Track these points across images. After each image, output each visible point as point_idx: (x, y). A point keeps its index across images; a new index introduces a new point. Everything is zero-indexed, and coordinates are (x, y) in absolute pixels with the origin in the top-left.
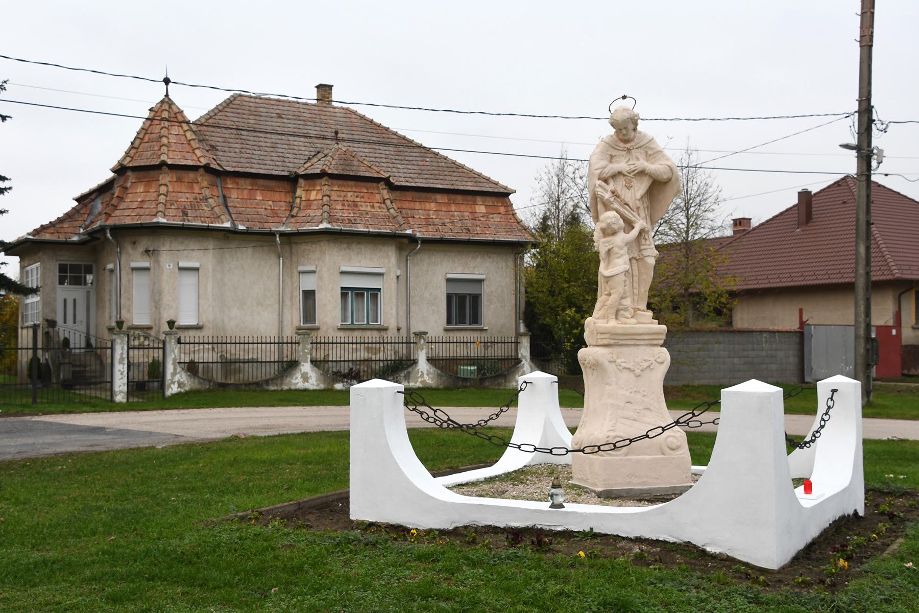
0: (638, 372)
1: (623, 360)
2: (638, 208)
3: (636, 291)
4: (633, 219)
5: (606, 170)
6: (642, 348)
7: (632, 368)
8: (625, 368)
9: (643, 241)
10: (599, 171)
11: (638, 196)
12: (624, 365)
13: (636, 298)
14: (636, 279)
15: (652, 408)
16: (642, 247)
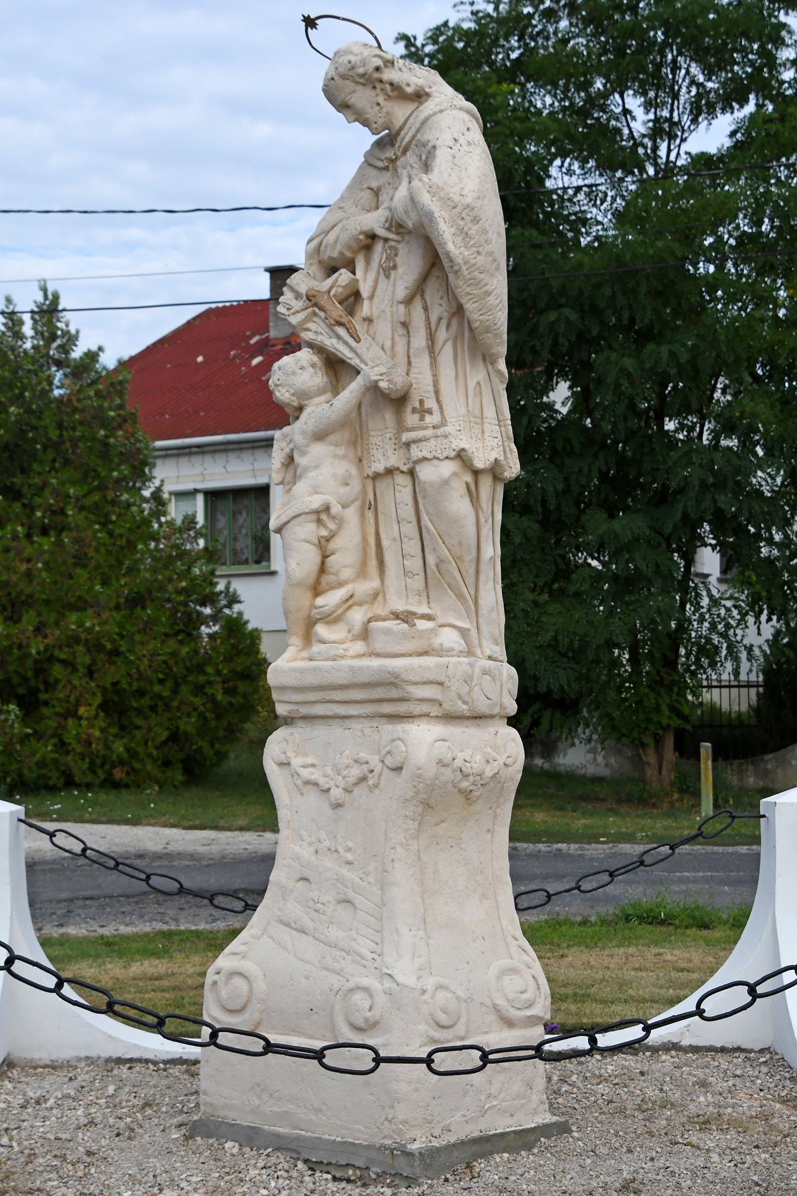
0: (336, 793)
1: (310, 760)
2: (405, 325)
3: (415, 564)
4: (355, 361)
5: (331, 237)
6: (356, 725)
7: (322, 781)
8: (307, 783)
9: (411, 419)
10: (315, 243)
11: (401, 293)
12: (306, 773)
13: (417, 583)
14: (410, 529)
15: (359, 900)
16: (406, 437)
